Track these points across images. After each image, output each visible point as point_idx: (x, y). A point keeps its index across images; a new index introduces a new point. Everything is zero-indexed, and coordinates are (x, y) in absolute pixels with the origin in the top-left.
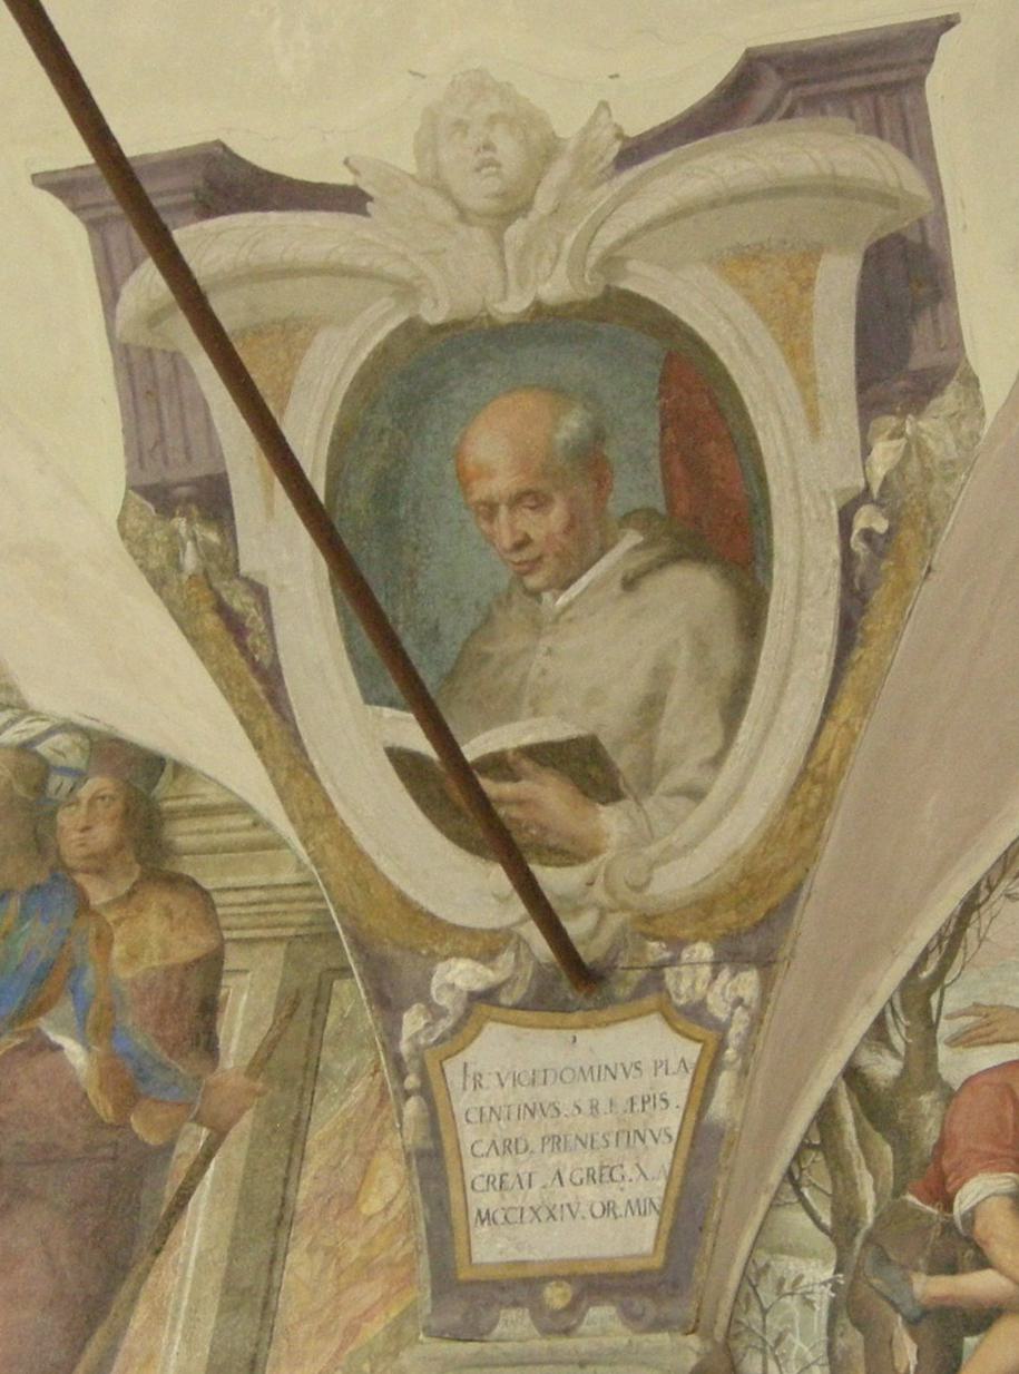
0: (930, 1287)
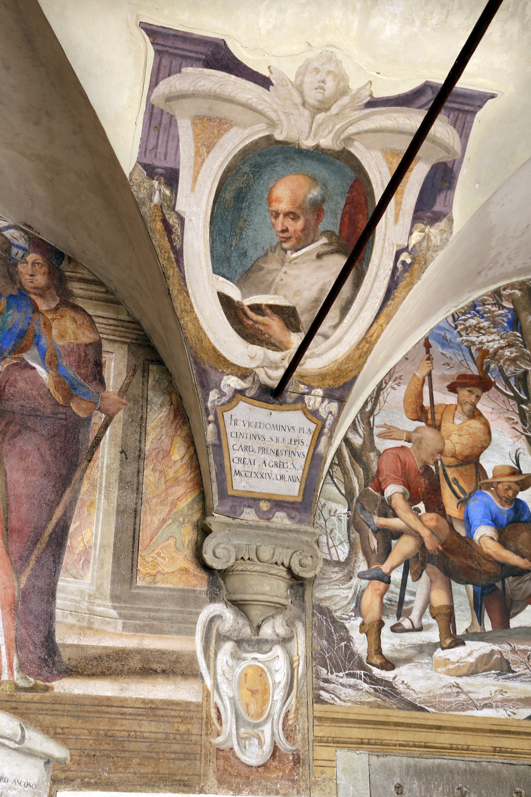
0: (379, 521)
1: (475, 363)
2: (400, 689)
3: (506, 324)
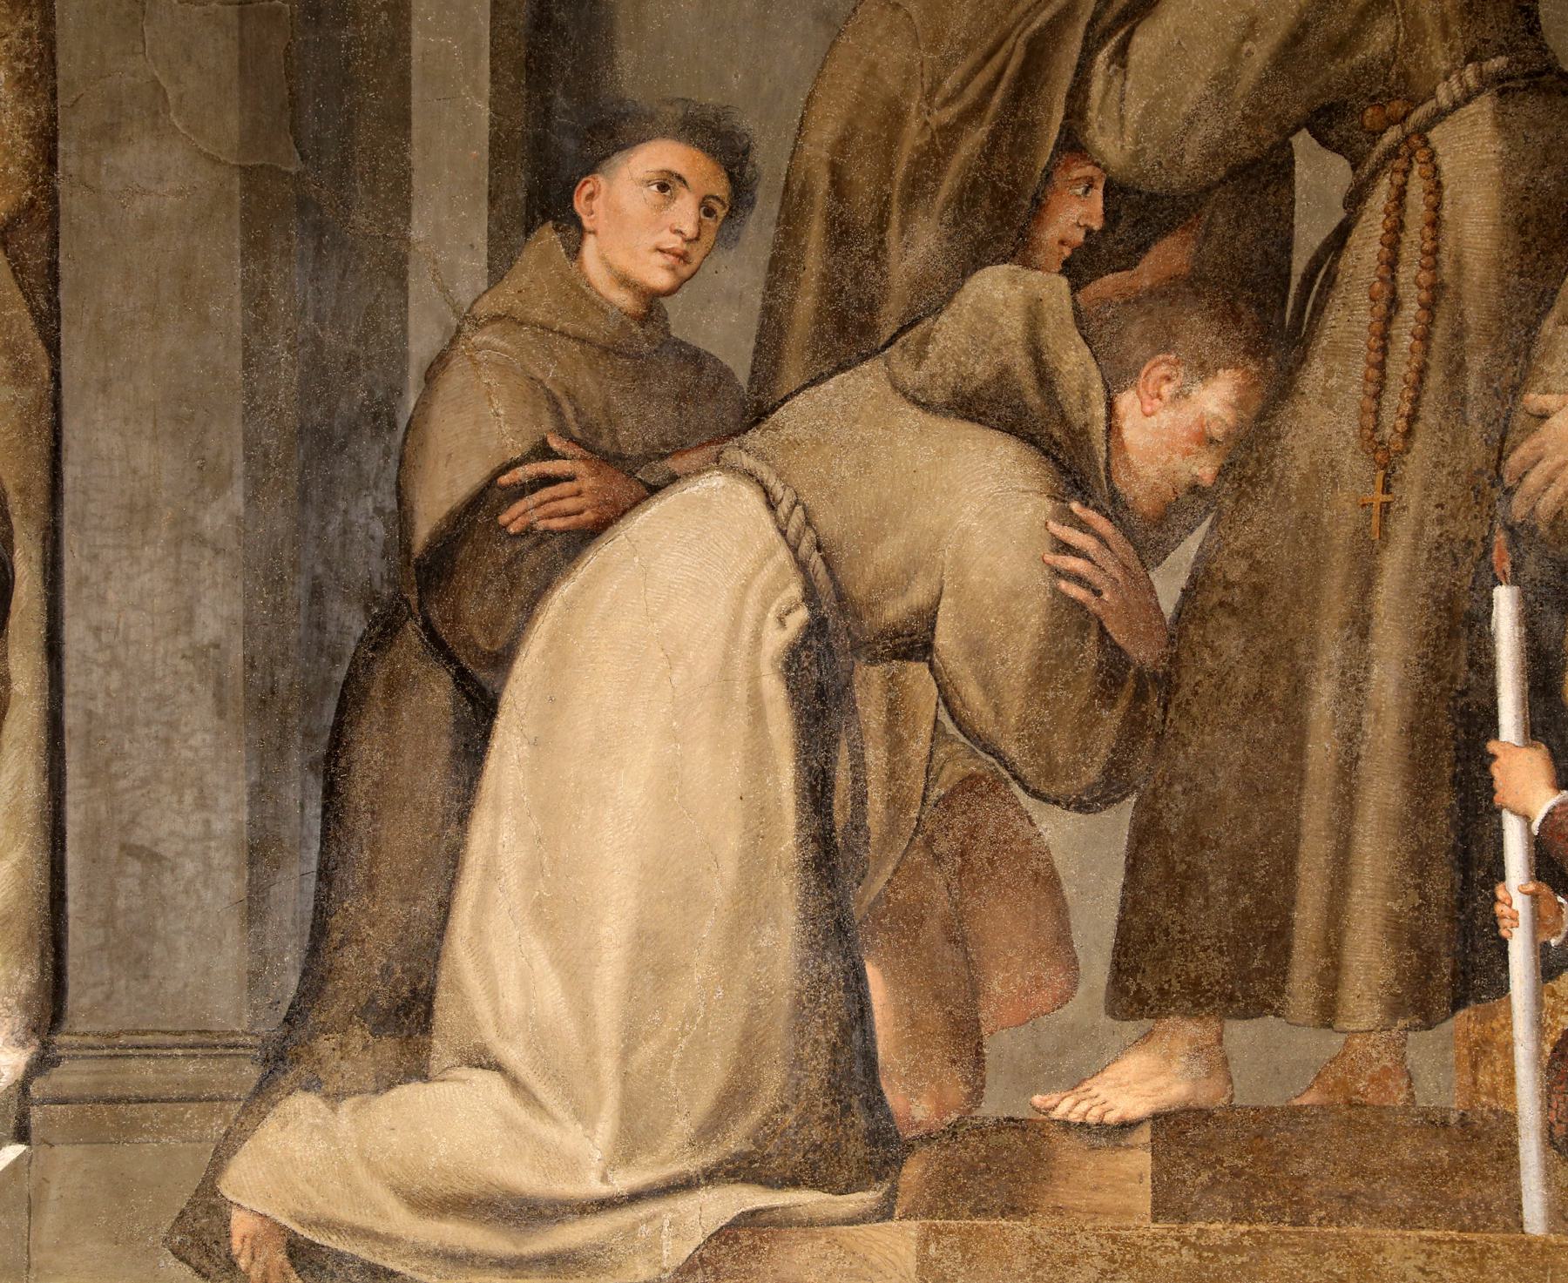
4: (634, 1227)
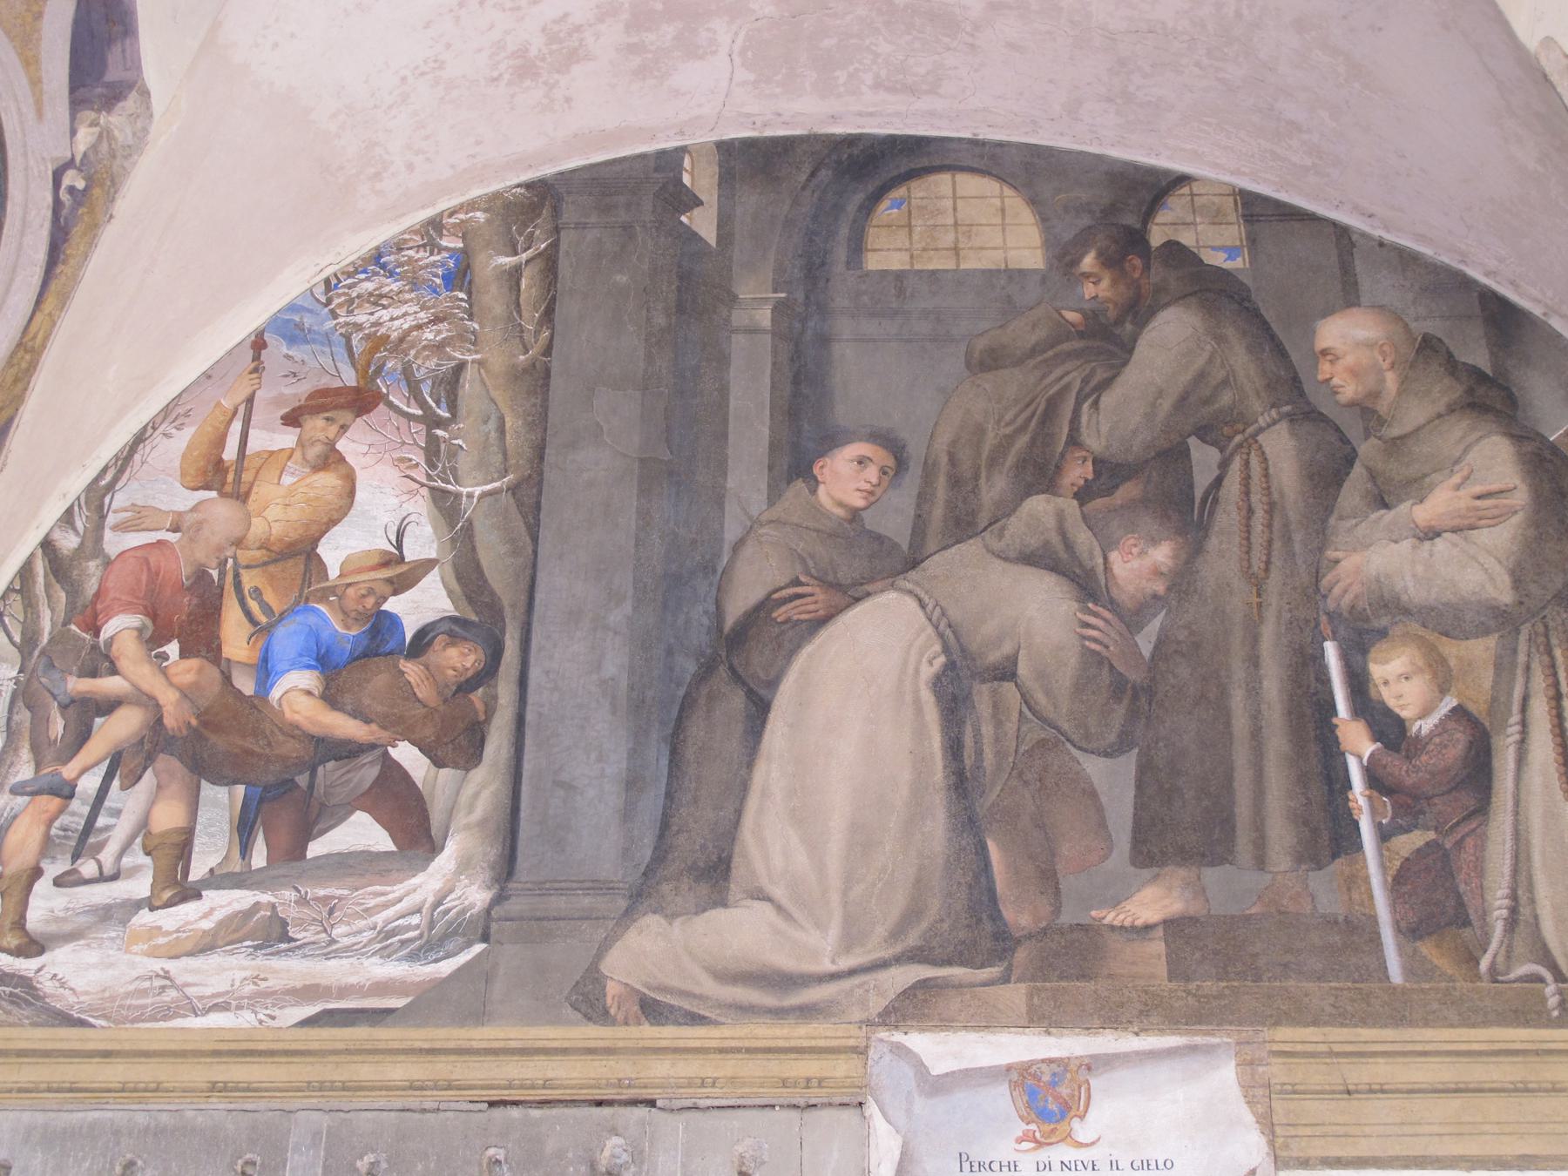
0: (78, 685)
1: (353, 365)
2: (48, 991)
3: (438, 281)
4: (852, 990)
